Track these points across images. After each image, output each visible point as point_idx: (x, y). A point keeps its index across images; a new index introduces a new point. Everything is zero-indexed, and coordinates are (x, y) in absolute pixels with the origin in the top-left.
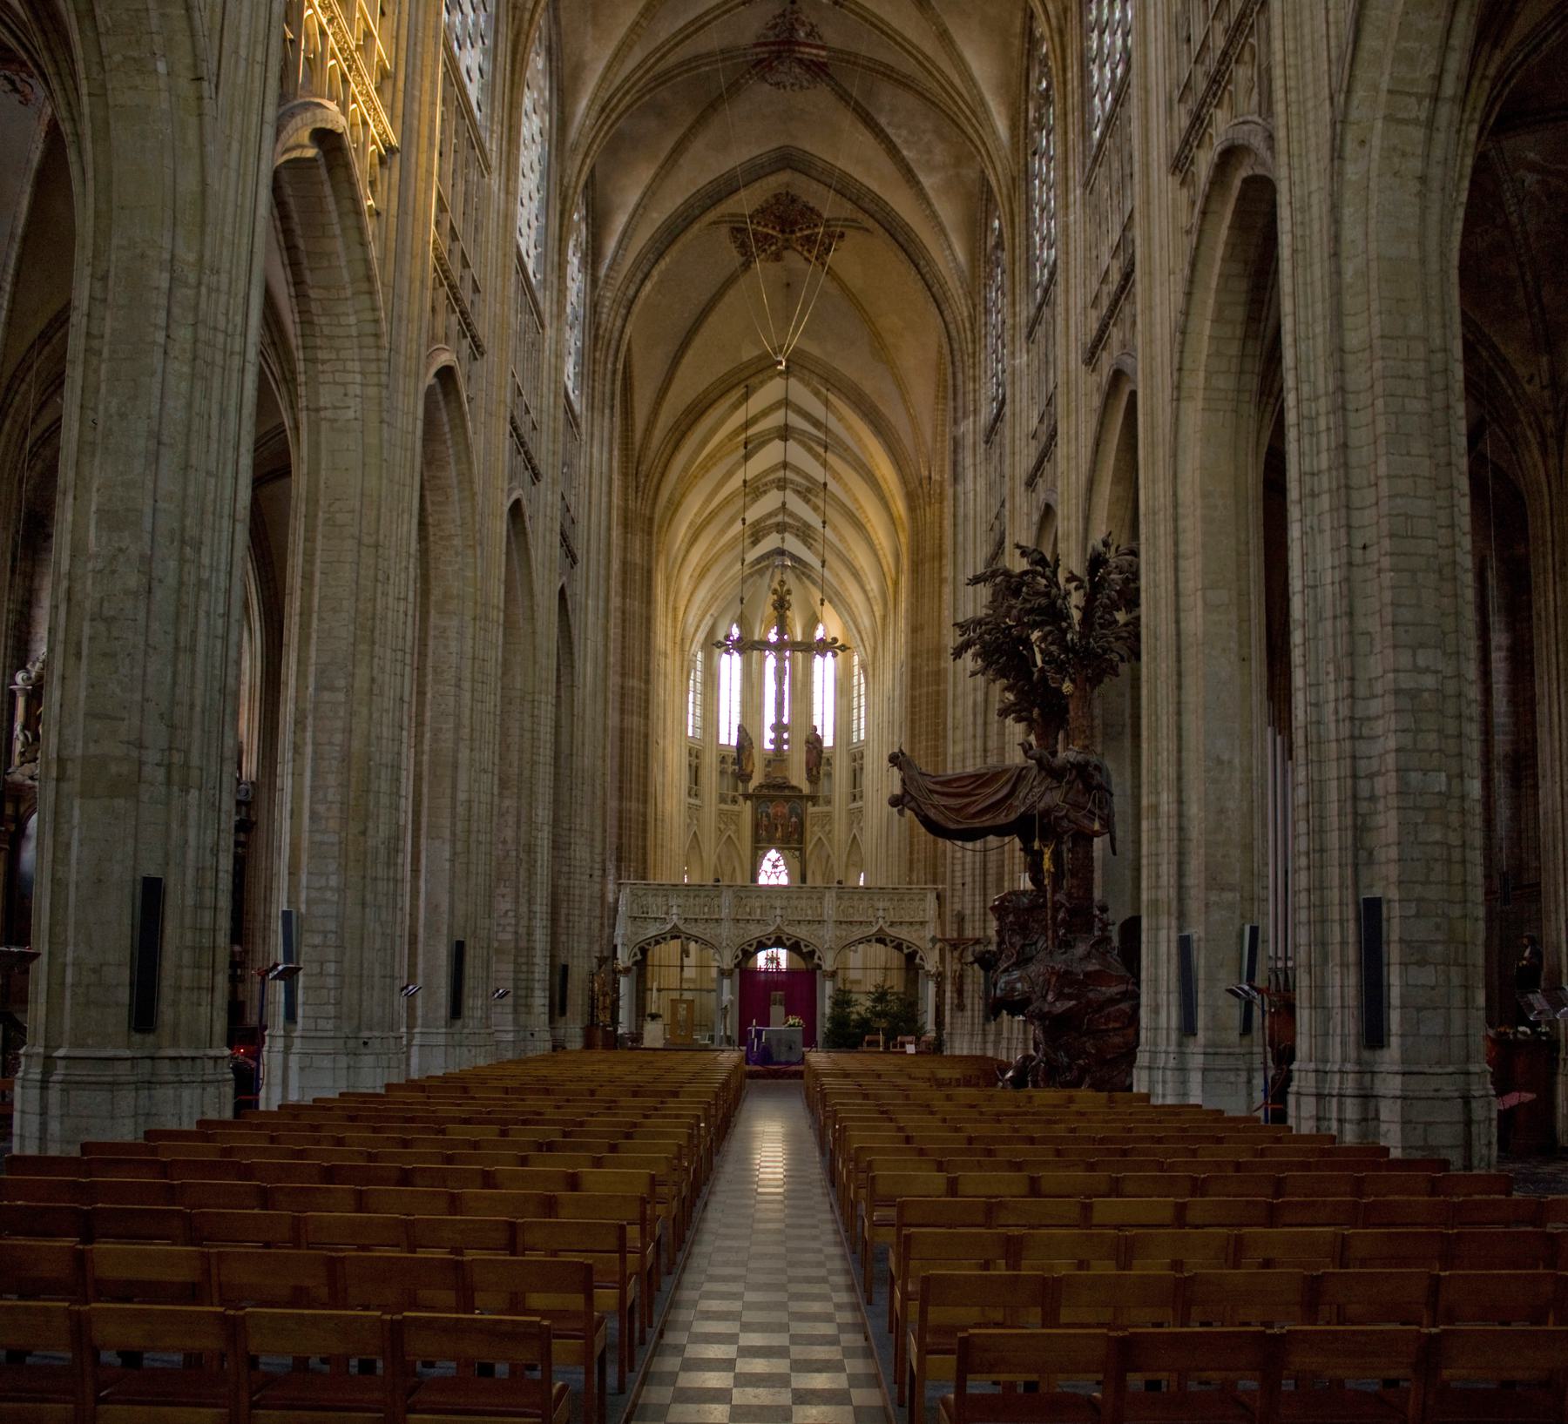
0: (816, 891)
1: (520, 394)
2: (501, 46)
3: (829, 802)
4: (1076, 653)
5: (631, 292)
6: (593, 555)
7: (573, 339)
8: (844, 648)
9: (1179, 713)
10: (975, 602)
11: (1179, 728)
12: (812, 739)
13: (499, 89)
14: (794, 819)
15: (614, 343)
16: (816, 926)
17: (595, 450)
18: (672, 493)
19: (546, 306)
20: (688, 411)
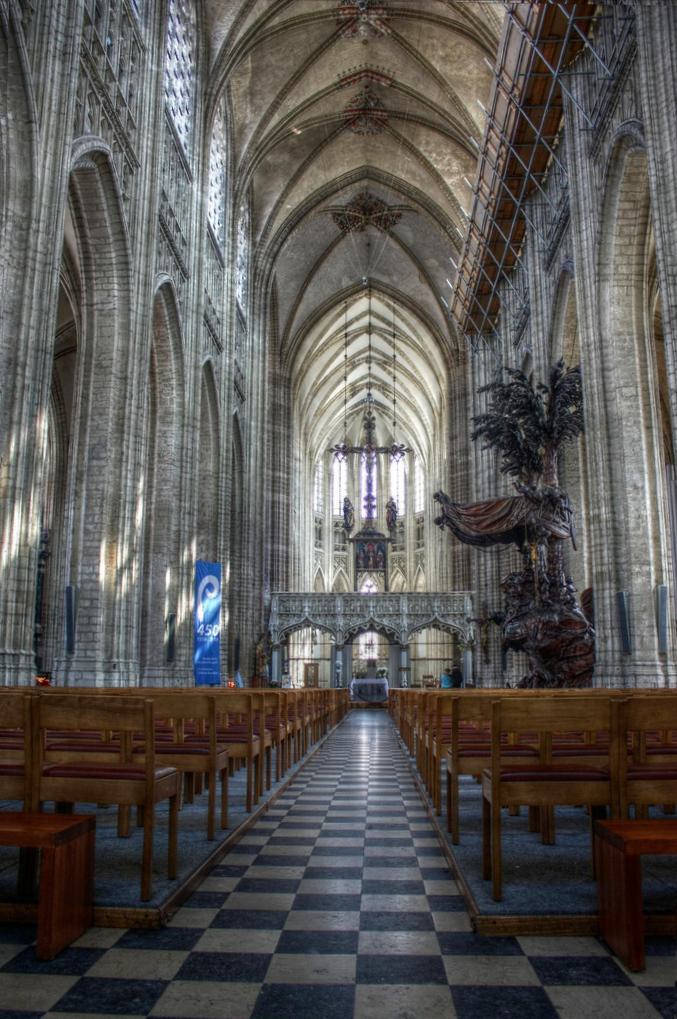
0: (397, 597)
1: (210, 303)
2: (198, 115)
3: (403, 549)
4: (545, 430)
5: (275, 249)
6: (254, 396)
7: (241, 275)
9: (610, 460)
10: (483, 404)
11: (610, 469)
13: (197, 137)
15: (265, 277)
17: (255, 337)
18: (302, 366)
19: (226, 255)
20: (310, 317)
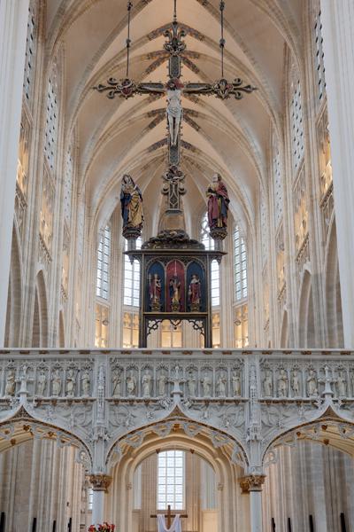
0: (234, 360)
8: (248, 89)
12: (214, 186)
14: (194, 281)
16: (232, 409)
